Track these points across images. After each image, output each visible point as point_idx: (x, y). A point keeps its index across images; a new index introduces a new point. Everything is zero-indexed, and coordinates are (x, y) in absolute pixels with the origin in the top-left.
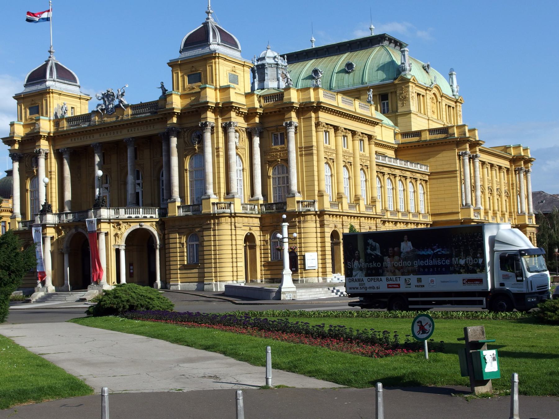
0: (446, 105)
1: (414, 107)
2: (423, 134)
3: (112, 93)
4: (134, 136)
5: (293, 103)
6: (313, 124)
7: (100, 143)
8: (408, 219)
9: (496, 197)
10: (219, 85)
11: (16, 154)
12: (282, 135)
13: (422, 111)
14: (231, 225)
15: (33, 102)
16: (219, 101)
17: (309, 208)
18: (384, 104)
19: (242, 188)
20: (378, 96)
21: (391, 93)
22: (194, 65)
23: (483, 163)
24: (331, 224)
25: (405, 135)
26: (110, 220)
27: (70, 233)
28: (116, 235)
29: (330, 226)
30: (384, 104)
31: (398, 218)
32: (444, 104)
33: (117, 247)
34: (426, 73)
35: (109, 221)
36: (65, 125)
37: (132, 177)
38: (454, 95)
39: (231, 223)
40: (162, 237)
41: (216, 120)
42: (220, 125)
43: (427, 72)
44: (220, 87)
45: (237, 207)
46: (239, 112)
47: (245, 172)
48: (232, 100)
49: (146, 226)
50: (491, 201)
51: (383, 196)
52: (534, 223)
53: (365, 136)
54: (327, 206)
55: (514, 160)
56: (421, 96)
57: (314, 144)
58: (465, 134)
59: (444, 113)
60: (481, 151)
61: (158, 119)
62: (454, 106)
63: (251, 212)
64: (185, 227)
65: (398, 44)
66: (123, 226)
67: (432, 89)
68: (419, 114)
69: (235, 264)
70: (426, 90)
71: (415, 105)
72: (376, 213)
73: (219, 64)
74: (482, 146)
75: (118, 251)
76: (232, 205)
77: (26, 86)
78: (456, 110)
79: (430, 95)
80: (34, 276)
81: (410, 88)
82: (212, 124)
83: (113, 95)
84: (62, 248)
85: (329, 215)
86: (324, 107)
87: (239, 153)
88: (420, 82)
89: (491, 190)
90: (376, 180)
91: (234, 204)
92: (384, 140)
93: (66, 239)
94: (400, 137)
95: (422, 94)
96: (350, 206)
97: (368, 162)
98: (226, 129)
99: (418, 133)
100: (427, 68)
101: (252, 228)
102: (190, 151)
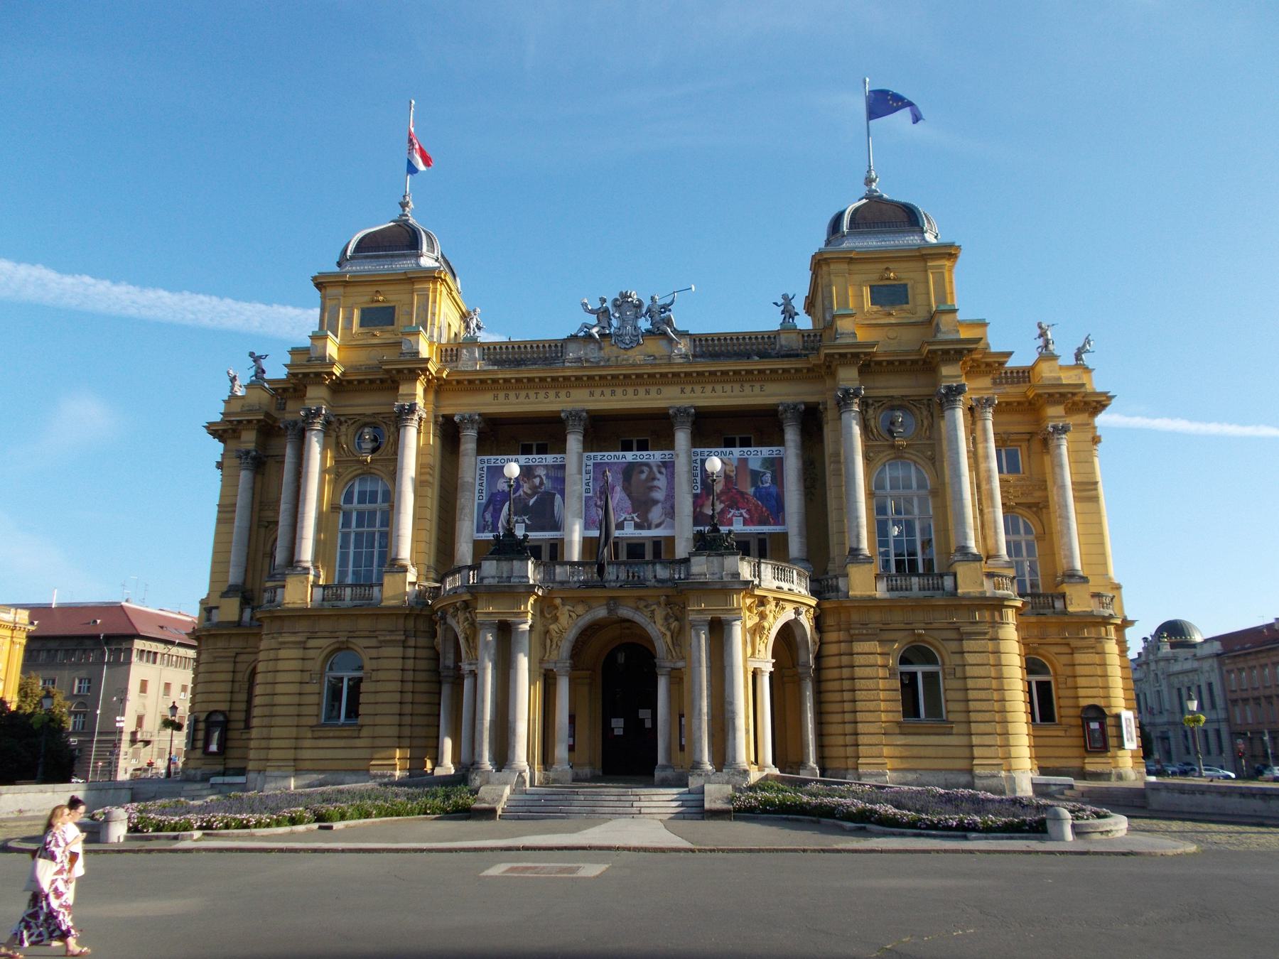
3: (639, 300)
4: (701, 403)
22: (891, 266)
61: (797, 370)
64: (902, 626)
80: (359, 737)
83: (640, 306)
93: (572, 634)
102: (883, 451)
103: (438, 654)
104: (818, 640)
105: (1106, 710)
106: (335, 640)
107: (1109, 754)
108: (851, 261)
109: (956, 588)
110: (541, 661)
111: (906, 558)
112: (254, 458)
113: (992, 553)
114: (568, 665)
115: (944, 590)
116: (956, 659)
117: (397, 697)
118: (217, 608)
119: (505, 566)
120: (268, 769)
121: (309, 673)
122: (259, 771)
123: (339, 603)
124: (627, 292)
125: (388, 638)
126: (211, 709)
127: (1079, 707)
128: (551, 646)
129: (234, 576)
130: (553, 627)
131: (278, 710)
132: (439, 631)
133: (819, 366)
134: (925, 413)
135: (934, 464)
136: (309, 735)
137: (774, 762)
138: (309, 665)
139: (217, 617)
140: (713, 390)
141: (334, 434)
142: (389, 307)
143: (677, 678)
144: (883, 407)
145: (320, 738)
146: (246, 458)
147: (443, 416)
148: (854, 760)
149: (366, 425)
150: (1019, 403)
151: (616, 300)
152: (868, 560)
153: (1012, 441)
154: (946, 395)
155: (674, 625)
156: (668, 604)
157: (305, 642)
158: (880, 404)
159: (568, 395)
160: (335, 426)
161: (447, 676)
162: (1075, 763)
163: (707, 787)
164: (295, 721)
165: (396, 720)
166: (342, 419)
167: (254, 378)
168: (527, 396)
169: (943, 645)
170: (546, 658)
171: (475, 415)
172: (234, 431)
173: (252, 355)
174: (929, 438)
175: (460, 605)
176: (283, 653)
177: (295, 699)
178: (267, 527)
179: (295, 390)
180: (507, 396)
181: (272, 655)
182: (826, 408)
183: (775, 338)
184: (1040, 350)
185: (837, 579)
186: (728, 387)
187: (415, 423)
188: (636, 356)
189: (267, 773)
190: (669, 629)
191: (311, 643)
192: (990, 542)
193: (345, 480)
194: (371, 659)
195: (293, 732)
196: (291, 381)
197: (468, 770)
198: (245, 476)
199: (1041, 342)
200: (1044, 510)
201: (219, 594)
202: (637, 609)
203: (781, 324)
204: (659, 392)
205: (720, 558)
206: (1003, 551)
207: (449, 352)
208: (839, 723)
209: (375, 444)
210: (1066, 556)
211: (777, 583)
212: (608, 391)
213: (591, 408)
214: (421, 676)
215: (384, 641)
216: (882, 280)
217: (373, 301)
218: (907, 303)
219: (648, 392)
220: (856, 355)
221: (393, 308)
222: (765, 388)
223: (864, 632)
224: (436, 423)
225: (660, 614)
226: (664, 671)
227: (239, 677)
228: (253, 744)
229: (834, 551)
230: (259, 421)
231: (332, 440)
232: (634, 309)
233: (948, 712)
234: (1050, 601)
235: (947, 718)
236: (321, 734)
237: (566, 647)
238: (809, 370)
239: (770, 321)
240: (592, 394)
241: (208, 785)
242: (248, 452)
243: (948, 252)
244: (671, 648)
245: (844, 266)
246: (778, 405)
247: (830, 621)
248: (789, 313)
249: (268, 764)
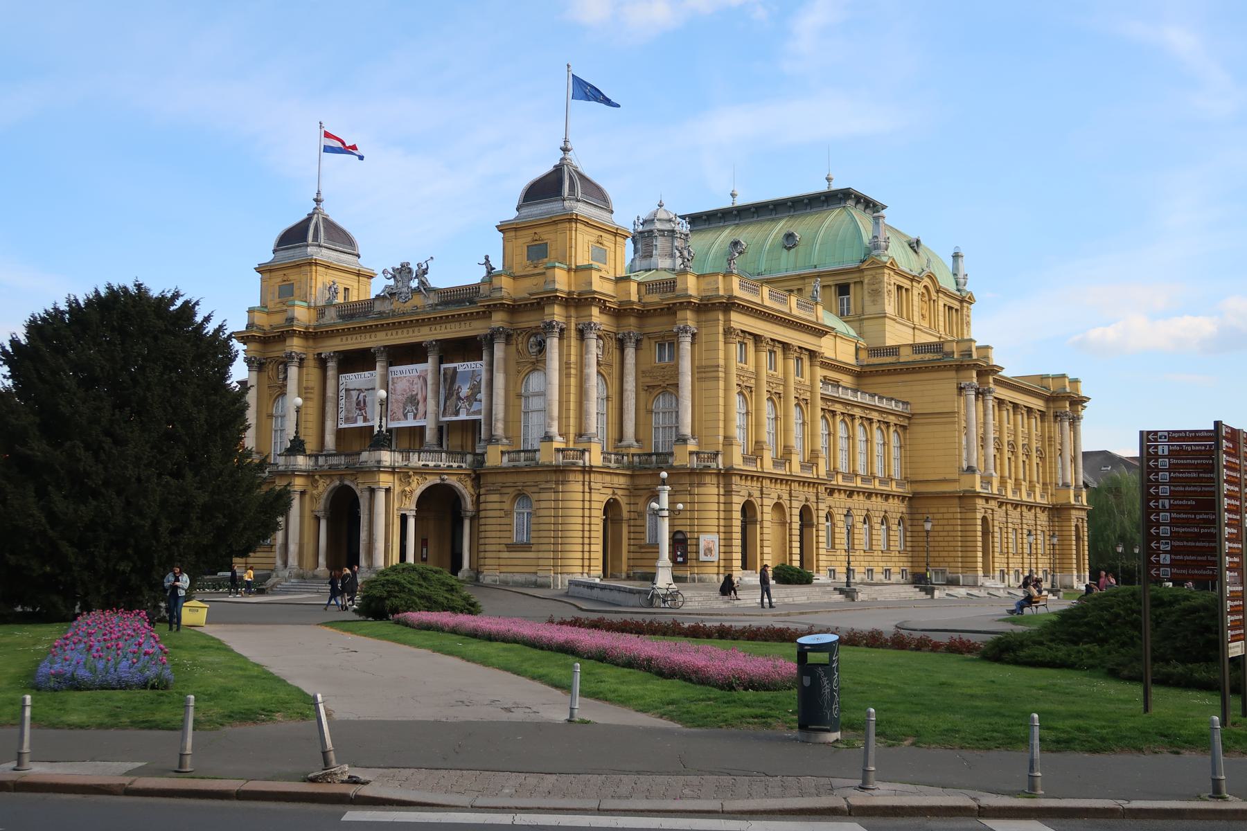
0: (945, 305)
1: (890, 308)
2: (902, 350)
5: (691, 296)
6: (721, 330)
7: (385, 347)
8: (872, 487)
9: (1021, 458)
10: (576, 263)
11: (255, 358)
12: (671, 344)
13: (903, 313)
14: (584, 485)
16: (573, 289)
17: (709, 464)
18: (842, 300)
19: (605, 427)
20: (833, 288)
21: (855, 283)
22: (537, 230)
23: (1000, 402)
24: (742, 491)
25: (875, 351)
26: (394, 468)
27: (332, 486)
28: (404, 491)
29: (741, 494)
30: (842, 300)
31: (854, 485)
32: (941, 304)
33: (403, 512)
34: (915, 254)
35: (393, 471)
36: (331, 316)
38: (958, 290)
39: (584, 482)
40: (474, 498)
41: (568, 317)
42: (573, 326)
43: (916, 252)
44: (576, 266)
45: (595, 457)
46: (606, 307)
47: (610, 403)
48: (595, 288)
49: (452, 480)
50: (1013, 464)
51: (831, 449)
52: (1085, 504)
53: (804, 352)
54: (738, 462)
55: (1051, 399)
56: (904, 290)
57: (721, 362)
58: (970, 355)
59: (941, 319)
60: (997, 382)
61: (478, 313)
62: (959, 308)
63: (616, 465)
65: (870, 205)
66: (415, 479)
67: (923, 279)
68: (899, 319)
69: (586, 547)
70: (912, 280)
71: (892, 304)
72: (818, 475)
73: (576, 230)
74: (1000, 373)
75: (404, 519)
76: (587, 454)
77: (275, 251)
78: (962, 315)
79: (918, 289)
81: (886, 277)
82: (561, 324)
85: (741, 476)
86: (739, 305)
87: (601, 371)
88: (902, 268)
89: (1013, 446)
90: (821, 426)
91: (590, 452)
92: (838, 359)
93: (325, 495)
94: (863, 355)
95: (906, 286)
96: (776, 463)
97: (809, 394)
98: (582, 334)
99: (894, 350)
100: (915, 245)
101: (616, 491)
180: (347, 339)
237: (322, 502)
239: (473, 275)
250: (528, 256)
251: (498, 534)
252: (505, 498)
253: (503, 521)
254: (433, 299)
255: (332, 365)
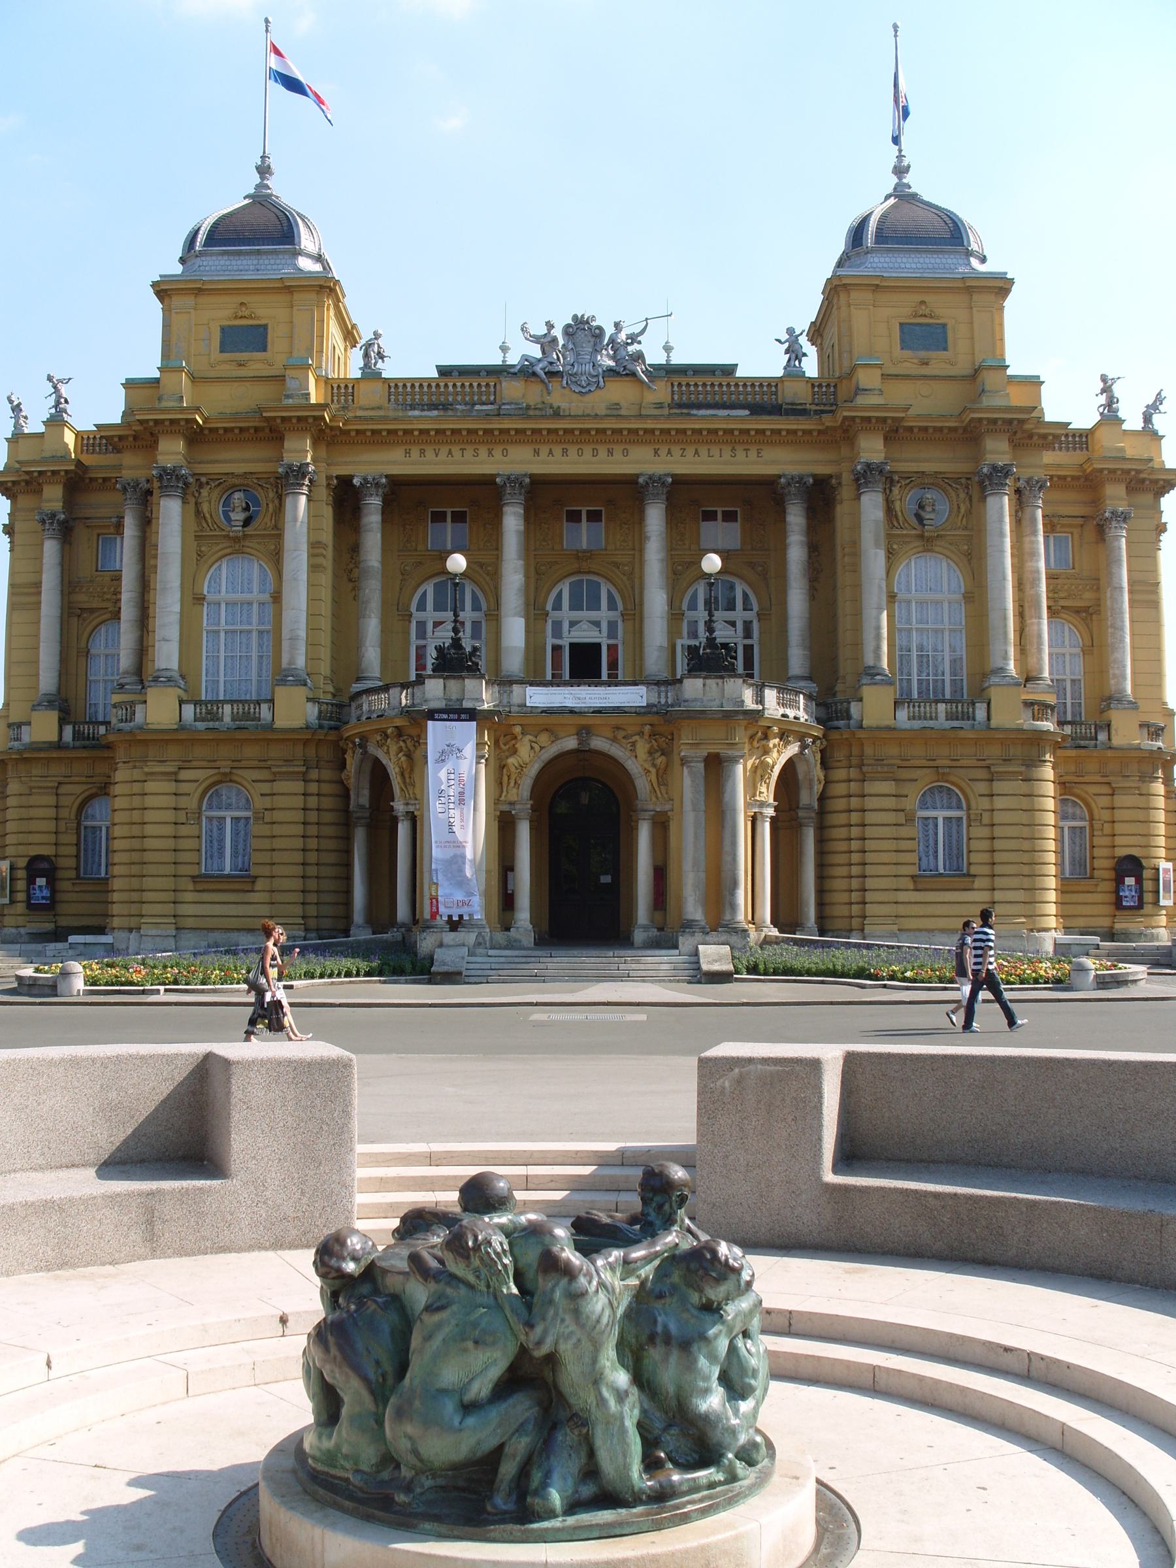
15: (247, 313)
22: (928, 298)
37: (665, 596)
80: (253, 891)
84: (513, 795)
93: (533, 770)
102: (909, 542)
103: (347, 790)
104: (823, 778)
105: (1144, 862)
106: (212, 772)
107: (1142, 912)
108: (877, 288)
109: (989, 719)
110: (497, 801)
111: (931, 678)
112: (60, 523)
113: (1034, 674)
114: (529, 806)
115: (974, 719)
116: (985, 803)
117: (299, 843)
118: (29, 724)
119: (453, 684)
120: (143, 926)
121: (184, 812)
122: (131, 930)
123: (217, 724)
124: (583, 316)
125: (284, 769)
126: (33, 853)
127: (1114, 858)
128: (509, 783)
129: (47, 681)
130: (512, 761)
131: (149, 857)
132: (352, 761)
133: (834, 429)
134: (962, 495)
135: (969, 561)
136: (191, 887)
137: (775, 922)
138: (183, 802)
139: (27, 736)
140: (696, 452)
141: (192, 500)
142: (260, 326)
143: (661, 826)
144: (911, 485)
145: (203, 891)
146: (52, 524)
147: (337, 477)
148: (860, 920)
149: (235, 488)
150: (1074, 478)
151: (568, 326)
152: (890, 683)
153: (1063, 526)
154: (989, 477)
155: (660, 760)
156: (653, 734)
157: (176, 774)
158: (908, 481)
159: (505, 453)
160: (193, 488)
161: (358, 818)
162: (1105, 922)
163: (701, 947)
164: (170, 870)
165: (299, 870)
166: (203, 479)
167: (53, 411)
168: (450, 452)
169: (968, 784)
170: (503, 798)
171: (381, 476)
172: (27, 483)
173: (50, 378)
174: (966, 528)
175: (392, 733)
176: (151, 786)
177: (170, 844)
178: (79, 616)
179: (135, 438)
180: (422, 452)
181: (137, 788)
182: (840, 484)
183: (776, 386)
184: (1101, 409)
185: (849, 703)
186: (715, 451)
187: (305, 490)
188: (599, 401)
189: (142, 932)
190: (654, 765)
191: (184, 775)
192: (1032, 661)
193: (210, 562)
194: (262, 795)
195: (169, 883)
196: (134, 428)
197: (409, 930)
198: (51, 549)
199: (1103, 399)
200: (1094, 617)
201: (30, 704)
202: (614, 740)
203: (785, 368)
204: (626, 453)
205: (720, 681)
206: (1046, 674)
207: (343, 391)
208: (843, 877)
209: (247, 514)
210: (1115, 676)
211: (781, 711)
212: (558, 451)
213: (536, 471)
214: (328, 817)
215: (279, 773)
216: (915, 316)
217: (236, 317)
218: (945, 349)
219: (610, 452)
220: (884, 420)
221: (265, 327)
222: (763, 453)
223: (879, 769)
224: (328, 485)
225: (642, 748)
226: (647, 815)
227: (64, 813)
228: (116, 897)
229: (845, 667)
230: (66, 472)
231: (192, 507)
232: (593, 340)
233: (969, 864)
234: (1093, 730)
235: (968, 870)
236: (206, 886)
237: (527, 783)
238: (820, 432)
240: (537, 452)
241: (66, 945)
242: (53, 516)
243: (1001, 286)
244: (655, 785)
245: (868, 296)
246: (780, 477)
247: (840, 754)
248: (794, 353)
249: (142, 921)
250: (902, 341)
251: (892, 857)
252: (907, 789)
253: (905, 832)
254: (661, 392)
255: (374, 503)
